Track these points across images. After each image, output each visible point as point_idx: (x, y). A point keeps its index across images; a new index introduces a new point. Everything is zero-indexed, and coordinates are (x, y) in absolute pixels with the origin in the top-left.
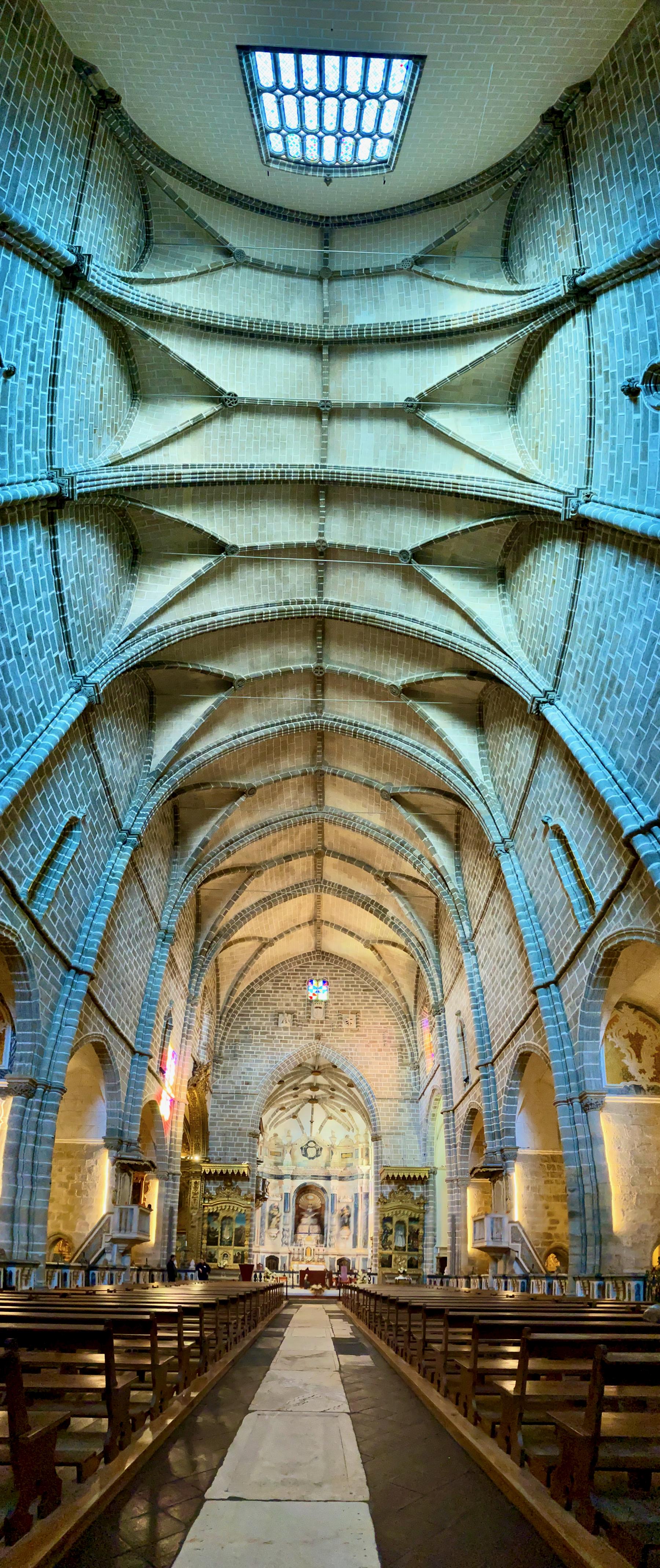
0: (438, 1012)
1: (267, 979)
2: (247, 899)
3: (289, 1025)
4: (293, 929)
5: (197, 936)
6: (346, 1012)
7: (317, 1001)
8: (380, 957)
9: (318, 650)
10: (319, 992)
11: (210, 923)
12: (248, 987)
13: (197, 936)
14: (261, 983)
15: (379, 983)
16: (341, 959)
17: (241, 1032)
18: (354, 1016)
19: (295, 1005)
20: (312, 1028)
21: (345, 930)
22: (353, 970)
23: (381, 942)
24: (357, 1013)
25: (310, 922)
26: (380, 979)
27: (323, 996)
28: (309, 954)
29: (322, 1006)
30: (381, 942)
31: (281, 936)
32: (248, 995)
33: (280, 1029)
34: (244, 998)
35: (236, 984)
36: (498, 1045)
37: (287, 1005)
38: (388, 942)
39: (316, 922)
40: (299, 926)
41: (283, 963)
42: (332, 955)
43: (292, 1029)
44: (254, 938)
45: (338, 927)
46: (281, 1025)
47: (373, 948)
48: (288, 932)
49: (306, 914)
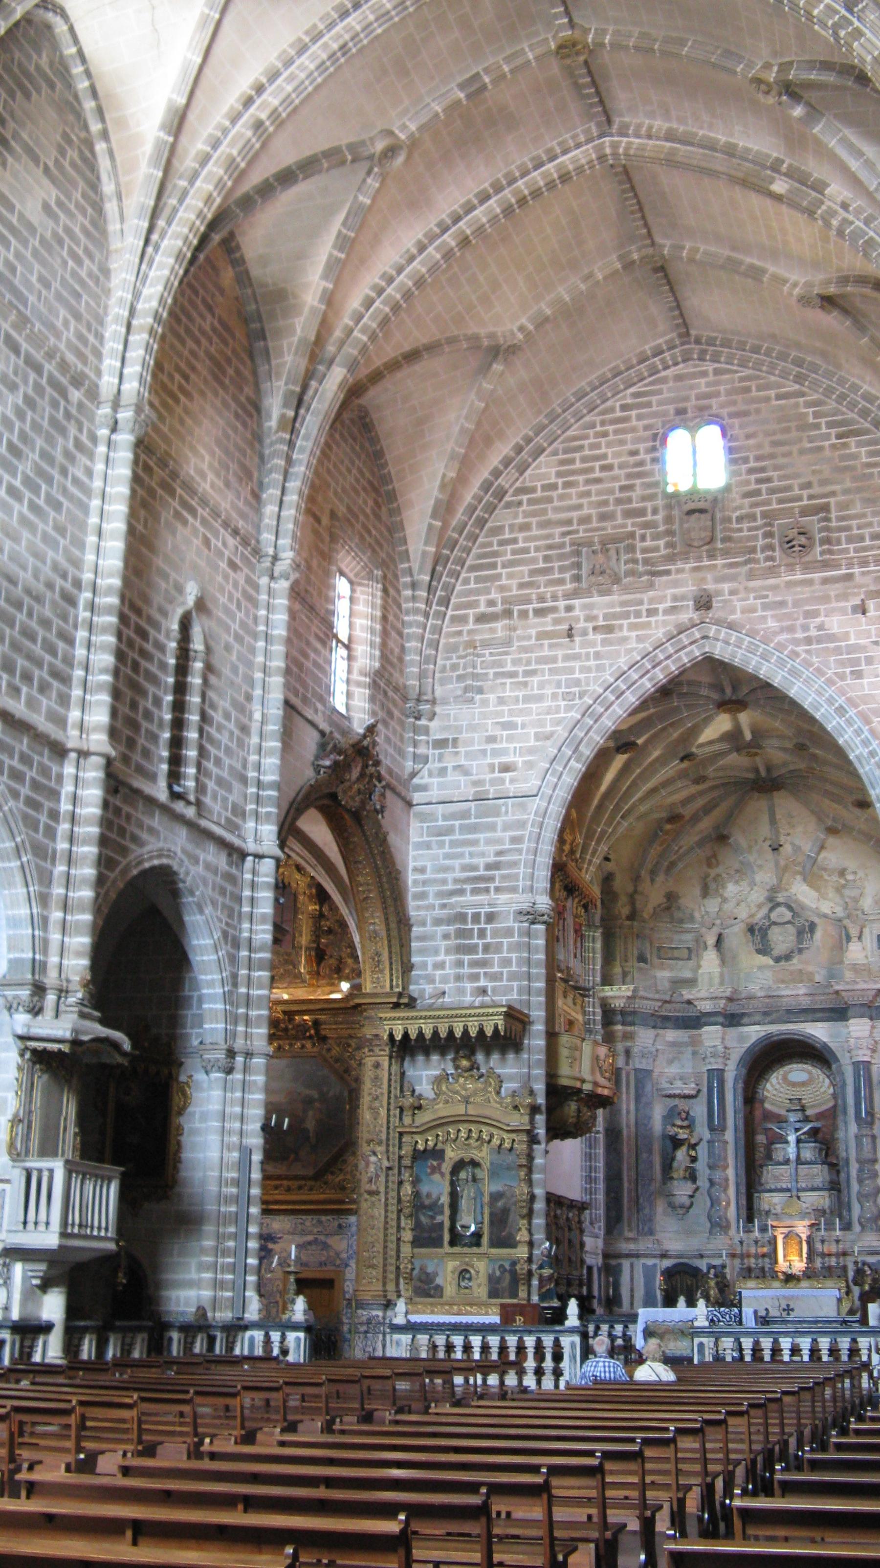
1: (539, 451)
12: (486, 486)
17: (481, 618)
19: (628, 514)
22: (799, 379)
30: (844, 280)
32: (491, 509)
37: (603, 517)
47: (828, 302)
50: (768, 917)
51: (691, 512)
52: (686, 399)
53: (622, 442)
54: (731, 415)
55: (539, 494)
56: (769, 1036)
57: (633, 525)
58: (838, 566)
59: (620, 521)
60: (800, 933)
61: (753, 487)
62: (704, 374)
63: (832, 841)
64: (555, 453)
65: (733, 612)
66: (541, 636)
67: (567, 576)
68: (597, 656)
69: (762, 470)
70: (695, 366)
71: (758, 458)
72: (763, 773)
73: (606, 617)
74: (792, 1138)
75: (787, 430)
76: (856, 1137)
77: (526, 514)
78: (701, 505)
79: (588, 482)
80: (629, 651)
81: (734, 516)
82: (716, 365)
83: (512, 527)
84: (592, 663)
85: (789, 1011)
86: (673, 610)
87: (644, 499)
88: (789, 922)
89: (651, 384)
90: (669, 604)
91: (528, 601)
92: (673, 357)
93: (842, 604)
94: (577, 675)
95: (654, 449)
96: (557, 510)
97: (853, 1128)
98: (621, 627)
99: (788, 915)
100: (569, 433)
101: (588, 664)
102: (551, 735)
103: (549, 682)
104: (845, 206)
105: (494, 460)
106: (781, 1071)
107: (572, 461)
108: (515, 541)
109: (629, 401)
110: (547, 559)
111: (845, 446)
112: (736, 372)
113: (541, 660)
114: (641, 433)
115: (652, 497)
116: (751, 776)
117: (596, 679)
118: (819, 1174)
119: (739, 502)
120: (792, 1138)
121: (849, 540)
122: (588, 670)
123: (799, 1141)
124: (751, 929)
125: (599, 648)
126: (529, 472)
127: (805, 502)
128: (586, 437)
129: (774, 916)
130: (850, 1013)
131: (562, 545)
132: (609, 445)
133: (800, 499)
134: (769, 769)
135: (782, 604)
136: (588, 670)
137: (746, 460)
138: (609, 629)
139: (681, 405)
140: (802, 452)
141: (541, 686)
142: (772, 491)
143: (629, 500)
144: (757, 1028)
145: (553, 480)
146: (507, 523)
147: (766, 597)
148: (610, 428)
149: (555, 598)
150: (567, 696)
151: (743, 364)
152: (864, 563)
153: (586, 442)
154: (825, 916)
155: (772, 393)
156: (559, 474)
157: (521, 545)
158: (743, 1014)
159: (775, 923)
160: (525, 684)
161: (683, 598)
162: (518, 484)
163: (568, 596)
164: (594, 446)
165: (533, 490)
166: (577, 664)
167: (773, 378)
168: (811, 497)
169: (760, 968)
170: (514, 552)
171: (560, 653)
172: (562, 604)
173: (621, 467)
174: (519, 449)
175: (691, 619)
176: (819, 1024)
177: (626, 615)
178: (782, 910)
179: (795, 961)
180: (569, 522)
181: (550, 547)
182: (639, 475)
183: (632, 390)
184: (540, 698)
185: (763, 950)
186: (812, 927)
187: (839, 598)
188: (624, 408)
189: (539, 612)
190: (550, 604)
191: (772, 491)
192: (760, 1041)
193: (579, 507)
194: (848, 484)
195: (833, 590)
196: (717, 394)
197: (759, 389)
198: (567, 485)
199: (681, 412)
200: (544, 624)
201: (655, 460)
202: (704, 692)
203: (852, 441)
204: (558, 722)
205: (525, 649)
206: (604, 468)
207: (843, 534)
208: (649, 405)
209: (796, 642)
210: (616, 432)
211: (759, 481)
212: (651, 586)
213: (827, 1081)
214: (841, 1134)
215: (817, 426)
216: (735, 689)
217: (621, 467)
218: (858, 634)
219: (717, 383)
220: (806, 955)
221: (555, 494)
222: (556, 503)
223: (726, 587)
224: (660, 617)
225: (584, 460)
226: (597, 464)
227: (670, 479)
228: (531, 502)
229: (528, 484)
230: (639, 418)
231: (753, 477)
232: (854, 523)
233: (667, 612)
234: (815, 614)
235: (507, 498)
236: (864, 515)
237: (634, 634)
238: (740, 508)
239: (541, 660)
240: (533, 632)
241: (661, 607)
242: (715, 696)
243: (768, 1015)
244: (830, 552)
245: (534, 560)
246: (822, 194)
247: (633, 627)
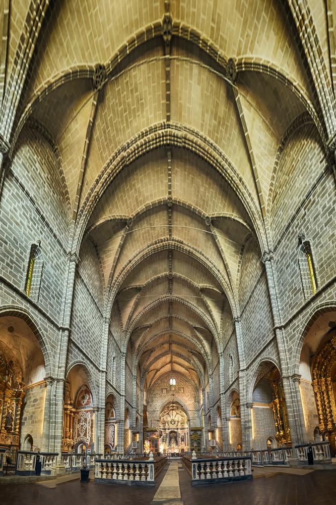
2: (152, 359)
4: (165, 365)
5: (140, 374)
9: (170, 261)
10: (173, 382)
11: (143, 367)
13: (140, 373)
20: (172, 393)
23: (190, 369)
25: (170, 363)
26: (190, 378)
34: (153, 385)
35: (151, 382)
38: (192, 369)
39: (171, 362)
49: (168, 360)
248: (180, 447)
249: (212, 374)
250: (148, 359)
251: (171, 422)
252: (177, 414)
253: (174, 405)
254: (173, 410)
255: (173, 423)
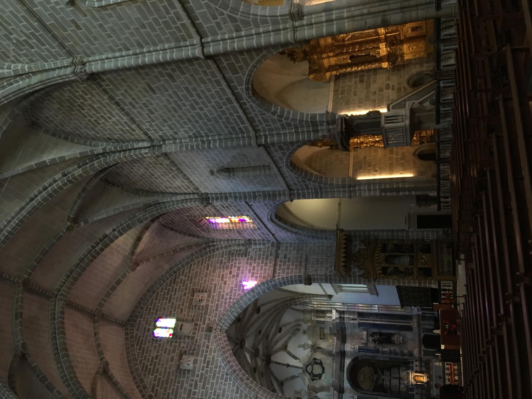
0: (207, 199)
1: (142, 381)
3: (192, 359)
6: (191, 300)
7: (174, 329)
8: (148, 260)
14: (145, 387)
15: (171, 269)
16: (139, 303)
18: (196, 294)
19: (174, 351)
21: (113, 288)
24: (193, 292)
27: (171, 322)
28: (126, 334)
29: (181, 323)
30: (133, 253)
31: (101, 353)
33: (195, 368)
36: (243, 123)
37: (172, 360)
40: (95, 334)
41: (129, 362)
42: (134, 311)
43: (197, 355)
44: (95, 378)
45: (108, 295)
46: (191, 367)
48: (99, 345)
50: (309, 374)
51: (181, 329)
52: (145, 328)
53: (151, 350)
54: (156, 314)
55: (156, 383)
56: (348, 378)
57: (178, 350)
58: (212, 287)
59: (175, 354)
60: (317, 363)
61: (180, 310)
62: (140, 321)
63: (289, 349)
64: (145, 375)
65: (215, 320)
66: (203, 388)
67: (187, 375)
68: (216, 367)
69: (175, 307)
70: (136, 324)
71: (172, 308)
72: (265, 358)
73: (204, 363)
74: (383, 377)
75: (167, 298)
76: (383, 354)
77: (161, 389)
78: (180, 325)
79: (159, 365)
80: (217, 357)
81: (186, 317)
82: (139, 317)
83: (164, 394)
84: (217, 370)
85: (340, 371)
86: (209, 340)
87: (171, 346)
88: (312, 366)
89: (136, 339)
90: (207, 341)
91: (190, 390)
92: (131, 330)
93: (222, 288)
94: (220, 376)
95: (157, 341)
96: (163, 377)
97: (379, 355)
98: (209, 358)
99: (310, 366)
100: (140, 369)
101: (217, 371)
102: (237, 387)
103: (220, 386)
104: (114, 230)
105: (140, 395)
106: (360, 383)
107: (150, 369)
108: (169, 393)
109: (138, 347)
110: (178, 383)
111: (177, 282)
112: (143, 312)
113: (211, 389)
114: (150, 344)
115: (172, 342)
116: (265, 362)
117: (224, 369)
118: (394, 370)
119: (183, 315)
120: (383, 377)
121: (205, 284)
122: (220, 371)
123: (383, 375)
124: (313, 380)
125: (214, 366)
126: (148, 386)
127: (190, 295)
128: (144, 363)
129: (310, 371)
130: (342, 349)
131: (176, 376)
132: (150, 356)
133: (188, 296)
134: (264, 356)
135: (217, 305)
136: (220, 371)
137: (171, 311)
138: (209, 362)
139: (147, 330)
140: (175, 295)
141: (220, 389)
142: (183, 305)
143: (170, 350)
144: (345, 383)
145: (154, 377)
146: (162, 396)
147: (214, 310)
148: (145, 354)
149: (192, 380)
150: (226, 381)
151: (142, 308)
152: (213, 280)
153: (146, 363)
154: (312, 354)
155: (154, 301)
156: (152, 375)
157: (171, 391)
158: (340, 386)
159: (312, 371)
160: (218, 395)
161: (206, 335)
162: (150, 390)
163: (194, 376)
164: (148, 362)
165: (154, 384)
166: (217, 375)
167: (150, 301)
168: (189, 293)
169: (325, 378)
170: (172, 395)
171: (211, 381)
172: (195, 378)
173: (158, 352)
174: (138, 387)
175: (214, 334)
176: (346, 361)
177: (206, 356)
178: (308, 369)
179: (325, 366)
180: (169, 372)
181: (175, 381)
182: (163, 346)
183: (135, 346)
184: (224, 390)
185: (320, 376)
186: (315, 359)
187: (220, 288)
188: (140, 350)
189: (196, 388)
190: (194, 383)
191: (183, 305)
192: (349, 382)
193: (166, 368)
194: (189, 282)
195: (217, 290)
196: (148, 318)
197: (151, 305)
198: (157, 372)
199: (149, 330)
200: (200, 385)
201: (160, 340)
202: (236, 348)
203: (177, 280)
204: (234, 384)
205: (206, 394)
206: (156, 359)
207: (203, 285)
208: (142, 340)
209: (230, 302)
210: (146, 353)
211: (178, 309)
212: (199, 346)
213: (364, 368)
214: (382, 359)
215: (169, 289)
216: (238, 340)
217: (158, 352)
218: (232, 284)
219: (145, 317)
220: (323, 362)
221: (158, 377)
222: (162, 377)
223: (207, 322)
224: (210, 344)
225: (151, 365)
226: (154, 360)
227: (168, 336)
228: (158, 386)
229: (151, 387)
230: (145, 344)
231: (177, 310)
232: (200, 282)
233: (209, 342)
234: (223, 295)
235: (153, 395)
236: (199, 279)
237: (213, 354)
238: (184, 316)
239: (211, 389)
240: (201, 390)
241: (207, 344)
242: (238, 346)
243: (341, 380)
244: (207, 289)
245: (178, 387)
246: (107, 236)
247: (210, 354)
248: (416, 352)
249: (151, 139)
250: (44, 379)
251: (315, 377)
252: (285, 347)
253: (248, 344)
254: (268, 360)
255: (317, 370)
